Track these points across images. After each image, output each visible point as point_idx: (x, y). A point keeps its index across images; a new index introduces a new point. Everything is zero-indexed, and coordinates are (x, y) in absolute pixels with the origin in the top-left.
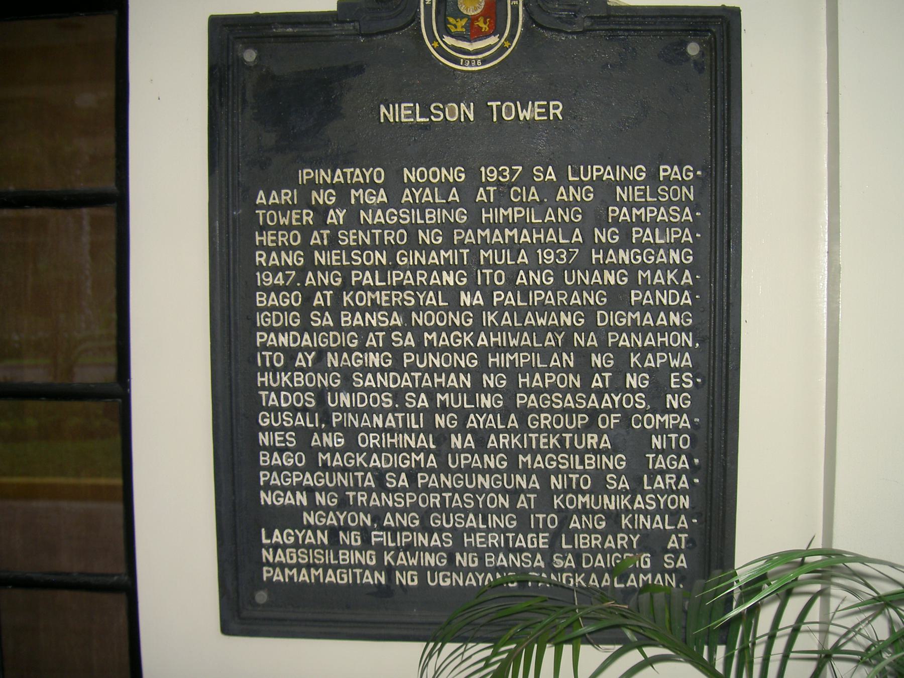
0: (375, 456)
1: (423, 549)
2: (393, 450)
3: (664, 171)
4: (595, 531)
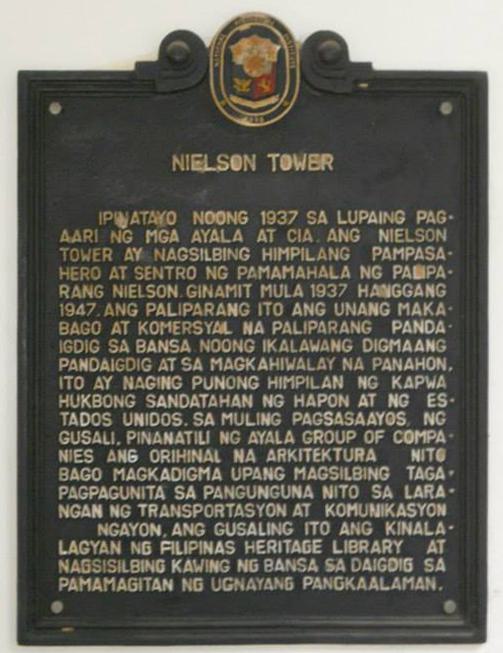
0: (165, 471)
1: (208, 556)
2: (182, 464)
3: (422, 215)
4: (362, 537)
